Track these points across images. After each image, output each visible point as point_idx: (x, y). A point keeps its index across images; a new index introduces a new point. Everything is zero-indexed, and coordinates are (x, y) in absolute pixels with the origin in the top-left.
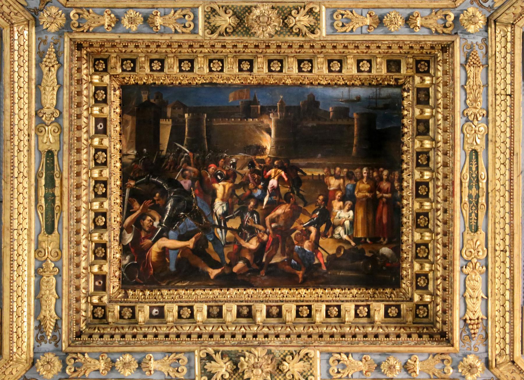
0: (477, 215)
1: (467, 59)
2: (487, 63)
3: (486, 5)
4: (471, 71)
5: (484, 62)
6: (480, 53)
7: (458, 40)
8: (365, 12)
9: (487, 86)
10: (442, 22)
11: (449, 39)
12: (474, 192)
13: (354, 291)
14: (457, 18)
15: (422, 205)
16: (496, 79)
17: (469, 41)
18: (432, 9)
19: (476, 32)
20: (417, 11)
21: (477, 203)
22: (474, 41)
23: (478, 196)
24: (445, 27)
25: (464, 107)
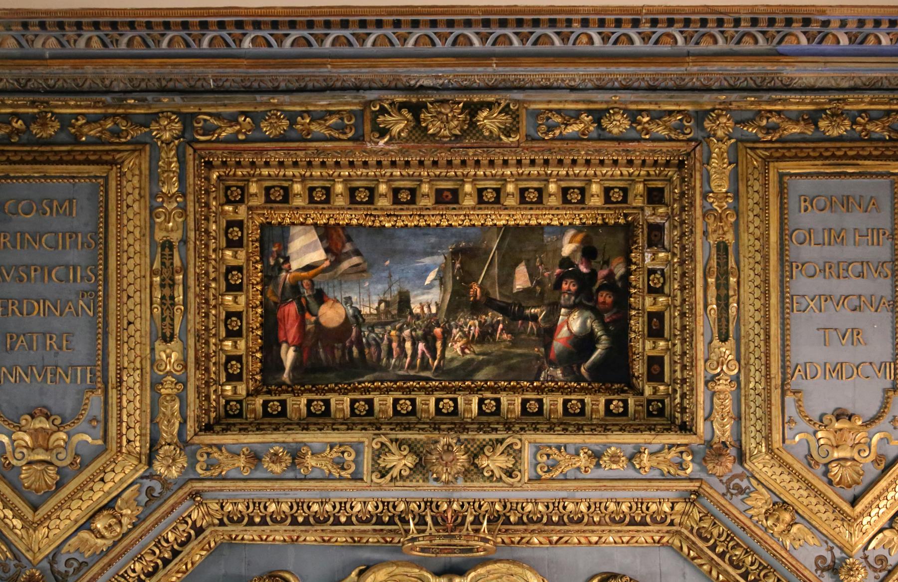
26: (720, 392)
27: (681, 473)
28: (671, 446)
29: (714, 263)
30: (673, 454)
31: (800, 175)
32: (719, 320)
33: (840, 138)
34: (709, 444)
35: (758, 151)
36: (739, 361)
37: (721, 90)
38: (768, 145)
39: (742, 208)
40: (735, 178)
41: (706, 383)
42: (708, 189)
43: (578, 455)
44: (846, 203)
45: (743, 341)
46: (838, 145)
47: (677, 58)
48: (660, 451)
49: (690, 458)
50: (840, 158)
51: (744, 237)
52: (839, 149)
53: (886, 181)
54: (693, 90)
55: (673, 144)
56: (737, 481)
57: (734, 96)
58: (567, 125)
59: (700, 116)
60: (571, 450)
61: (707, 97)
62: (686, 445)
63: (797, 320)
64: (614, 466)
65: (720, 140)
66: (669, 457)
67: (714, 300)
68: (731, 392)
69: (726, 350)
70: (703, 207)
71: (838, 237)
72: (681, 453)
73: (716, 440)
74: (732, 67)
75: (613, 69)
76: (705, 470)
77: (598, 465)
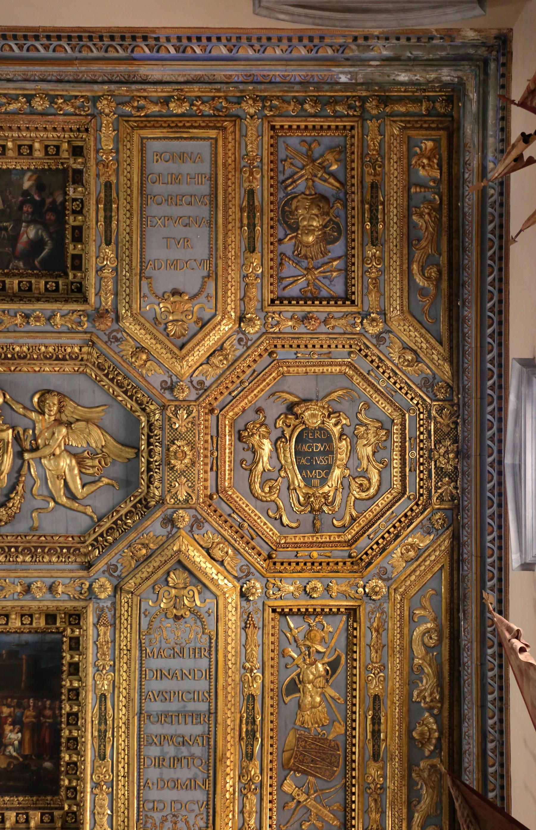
0: (105, 746)
1: (99, 620)
2: (115, 623)
3: (115, 574)
4: (102, 629)
5: (112, 622)
6: (109, 615)
7: (91, 605)
8: (17, 580)
9: (114, 641)
10: (79, 589)
11: (83, 604)
12: (103, 727)
13: (21, 799)
14: (91, 585)
15: (70, 732)
16: (120, 637)
17: (101, 605)
18: (71, 578)
19: (105, 598)
20: (60, 580)
21: (105, 736)
22: (105, 605)
23: (106, 731)
24: (81, 593)
25: (95, 659)
26: (105, 278)
27: (80, 328)
28: (73, 312)
29: (102, 195)
30: (75, 317)
31: (154, 138)
32: (106, 232)
33: (183, 115)
34: (97, 310)
35: (130, 123)
36: (117, 258)
37: (103, 83)
38: (137, 119)
39: (121, 160)
40: (117, 140)
41: (97, 272)
42: (99, 147)
43: (16, 316)
44: (182, 157)
45: (120, 245)
46: (181, 119)
47: (69, 61)
48: (67, 314)
49: (86, 319)
50: (180, 127)
51: (121, 178)
52: (180, 122)
53: (207, 143)
54: (85, 82)
55: (77, 117)
56: (115, 334)
57: (113, 87)
58: (9, 104)
59: (96, 99)
60: (12, 313)
61: (96, 87)
62: (83, 311)
63: (150, 230)
64: (38, 324)
65: (107, 115)
66: (73, 318)
67: (102, 219)
68: (112, 278)
69: (109, 252)
70: (96, 159)
71: (176, 179)
72: (80, 316)
73: (102, 308)
74: (108, 68)
75: (31, 68)
76: (94, 327)
77: (28, 323)
